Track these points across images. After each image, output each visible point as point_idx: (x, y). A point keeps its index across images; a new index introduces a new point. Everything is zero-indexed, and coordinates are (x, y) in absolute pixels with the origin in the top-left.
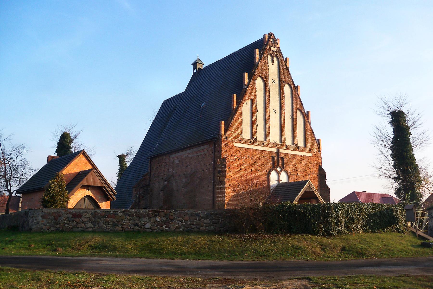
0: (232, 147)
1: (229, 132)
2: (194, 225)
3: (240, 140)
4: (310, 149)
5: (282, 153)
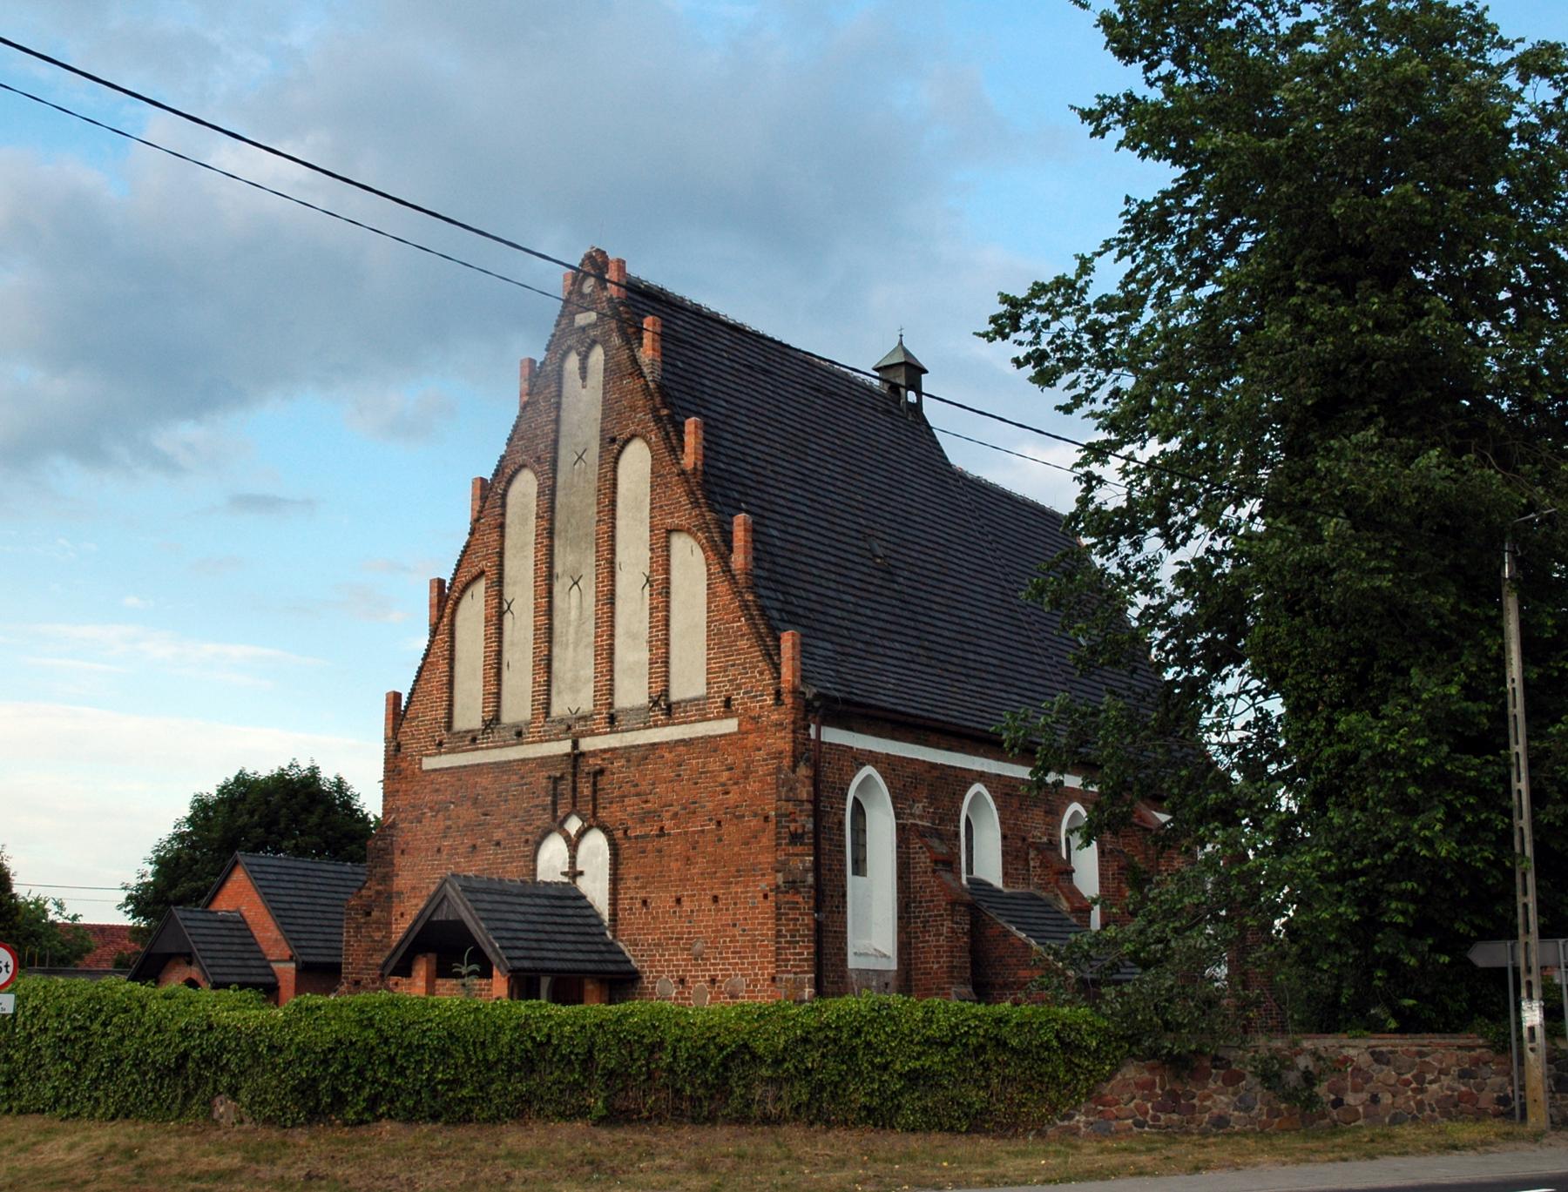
4: (728, 702)
5: (594, 754)
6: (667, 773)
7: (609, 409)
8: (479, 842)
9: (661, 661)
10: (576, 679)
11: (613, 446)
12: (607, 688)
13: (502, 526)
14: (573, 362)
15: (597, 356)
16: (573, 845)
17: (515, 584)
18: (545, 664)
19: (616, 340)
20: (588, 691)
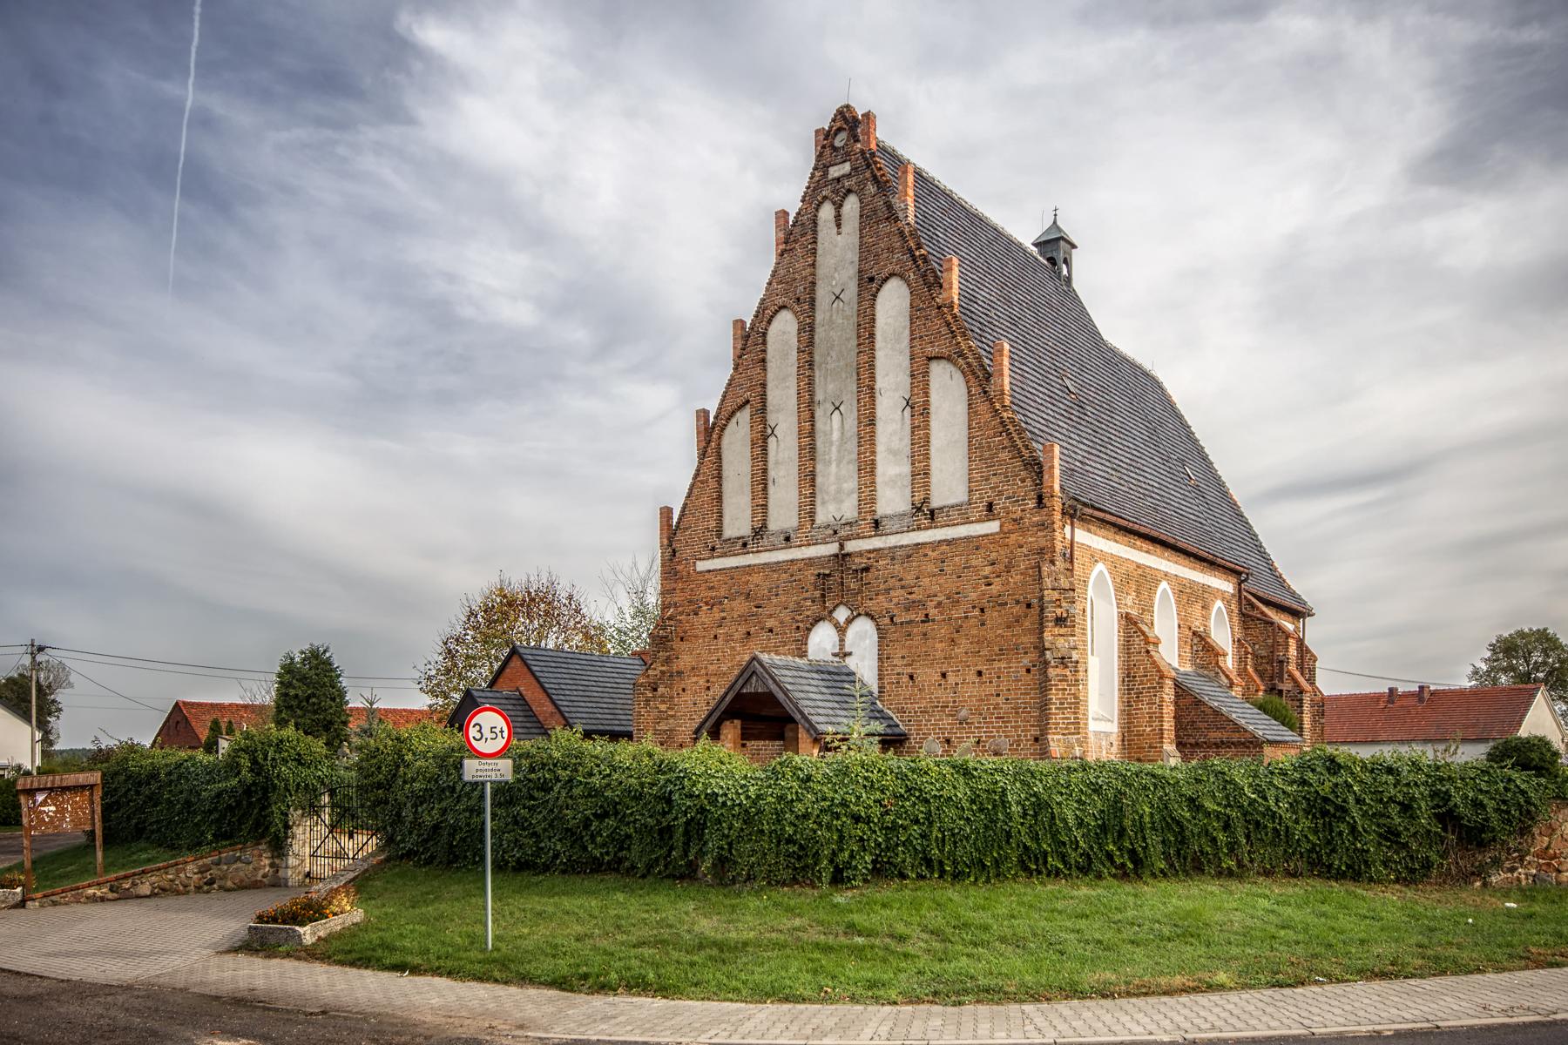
3: (713, 549)
4: (990, 507)
5: (860, 554)
6: (931, 568)
7: (865, 251)
8: (752, 630)
9: (921, 473)
10: (839, 491)
11: (870, 284)
12: (867, 497)
13: (764, 360)
14: (827, 212)
15: (851, 205)
16: (841, 630)
17: (778, 411)
18: (809, 478)
19: (871, 188)
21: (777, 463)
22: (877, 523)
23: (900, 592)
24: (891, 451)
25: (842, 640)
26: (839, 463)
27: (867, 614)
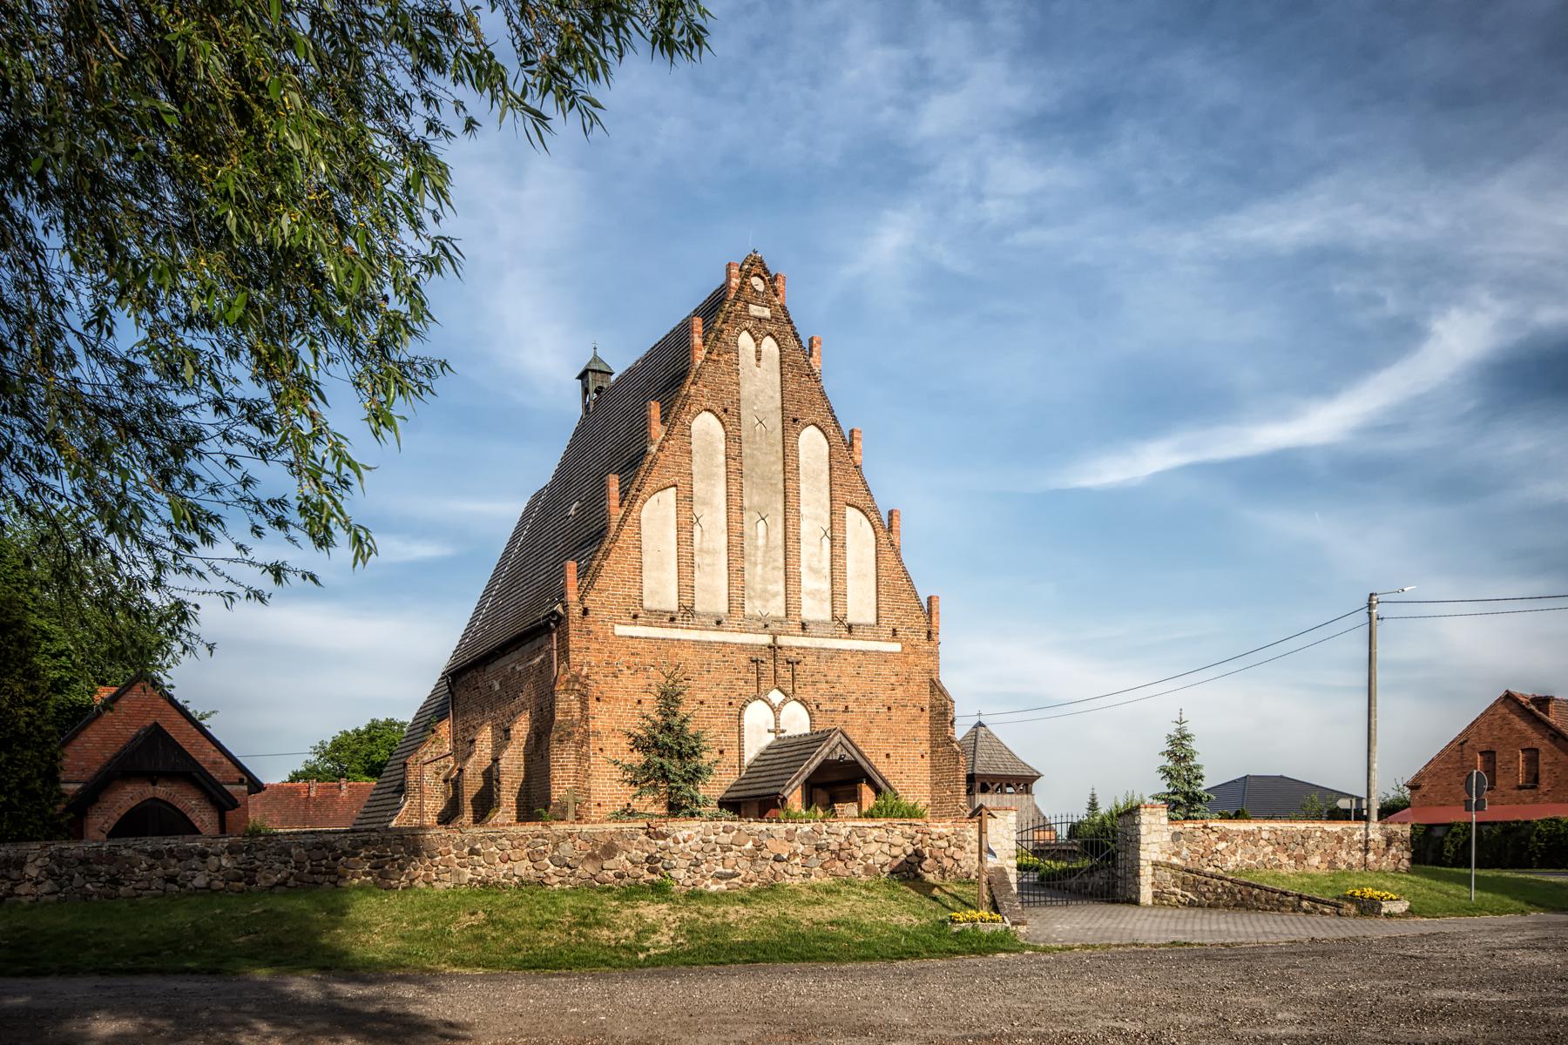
0: (609, 639)
1: (592, 595)
2: (320, 873)
3: (635, 617)
5: (790, 648)
9: (837, 595)
17: (704, 503)
18: (736, 571)
20: (781, 600)
21: (701, 550)
22: (804, 626)
23: (824, 686)
24: (811, 569)
25: (777, 720)
26: (765, 565)
27: (802, 702)
